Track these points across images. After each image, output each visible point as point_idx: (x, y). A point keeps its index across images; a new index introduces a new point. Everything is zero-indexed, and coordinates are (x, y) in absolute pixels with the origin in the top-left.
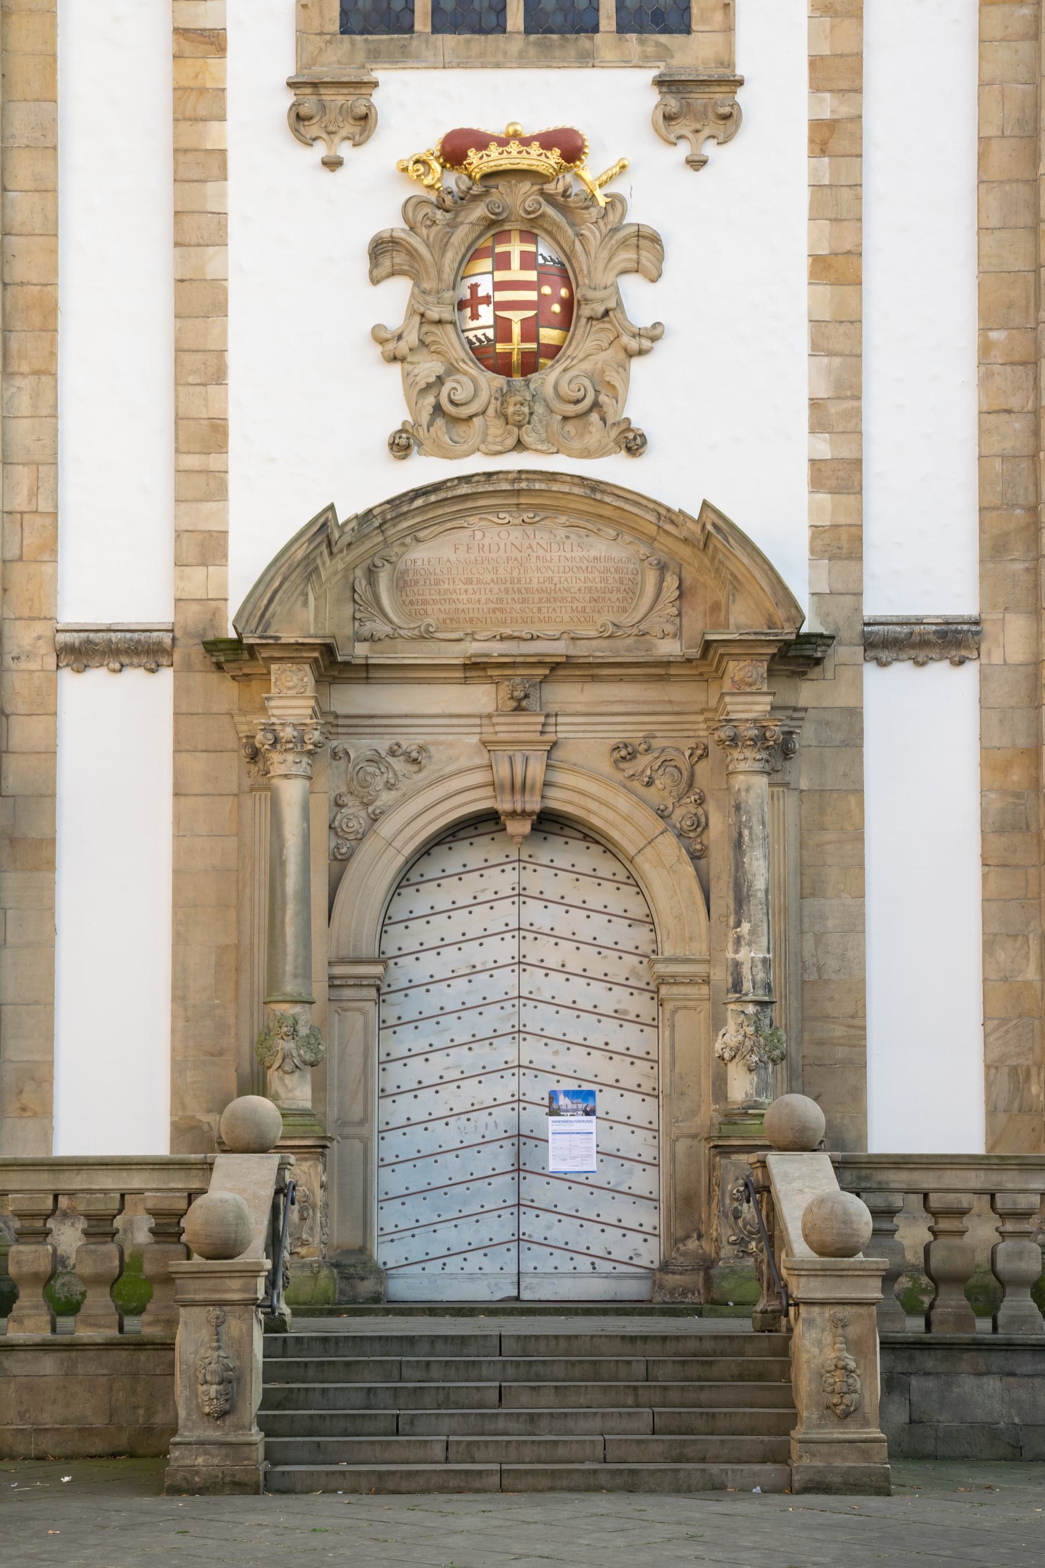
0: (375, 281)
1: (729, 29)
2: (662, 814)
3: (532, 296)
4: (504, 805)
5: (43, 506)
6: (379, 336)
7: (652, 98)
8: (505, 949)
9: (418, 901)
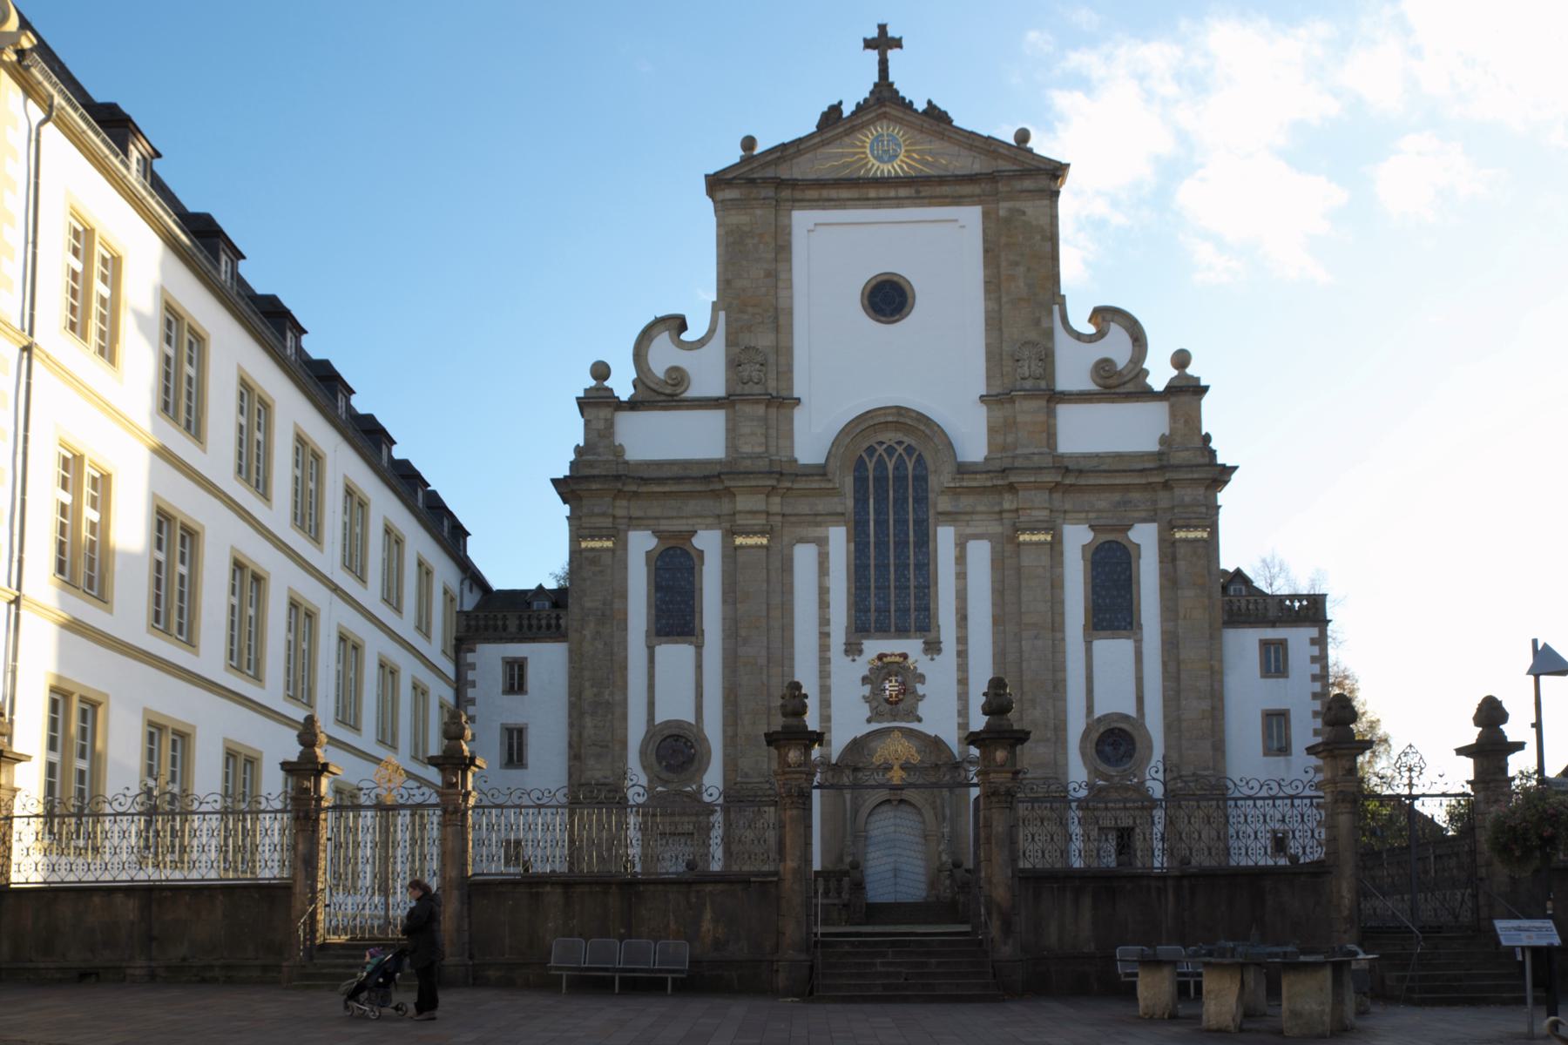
1: (939, 631)
2: (926, 800)
4: (892, 798)
6: (864, 697)
8: (892, 829)
9: (873, 819)
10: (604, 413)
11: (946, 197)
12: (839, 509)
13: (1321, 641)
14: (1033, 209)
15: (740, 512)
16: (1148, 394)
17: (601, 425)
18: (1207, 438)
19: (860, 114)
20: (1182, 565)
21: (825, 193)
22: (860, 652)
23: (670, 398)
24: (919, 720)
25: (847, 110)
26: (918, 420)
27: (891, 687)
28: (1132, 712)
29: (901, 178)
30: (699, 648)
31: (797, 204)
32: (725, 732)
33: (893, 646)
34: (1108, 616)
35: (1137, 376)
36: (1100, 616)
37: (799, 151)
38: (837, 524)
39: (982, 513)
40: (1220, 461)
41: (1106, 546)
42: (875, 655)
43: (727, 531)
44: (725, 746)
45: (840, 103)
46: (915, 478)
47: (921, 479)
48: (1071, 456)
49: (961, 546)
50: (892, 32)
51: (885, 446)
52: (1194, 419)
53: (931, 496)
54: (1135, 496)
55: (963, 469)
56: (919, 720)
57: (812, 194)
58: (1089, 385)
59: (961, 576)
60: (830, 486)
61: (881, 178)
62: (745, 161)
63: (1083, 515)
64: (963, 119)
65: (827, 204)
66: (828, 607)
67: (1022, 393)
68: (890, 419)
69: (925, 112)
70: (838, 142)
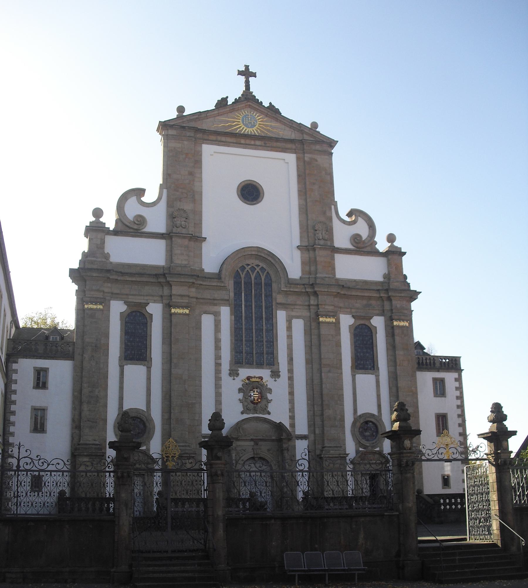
0: (239, 393)
3: (258, 396)
5: (200, 419)
6: (239, 400)
7: (270, 373)
10: (100, 235)
11: (279, 148)
12: (226, 297)
13: (459, 380)
14: (321, 159)
15: (174, 295)
16: (376, 253)
17: (99, 242)
18: (405, 277)
19: (237, 104)
20: (397, 338)
21: (219, 138)
22: (238, 375)
23: (136, 231)
24: (269, 413)
25: (230, 101)
26: (269, 255)
27: (255, 394)
28: (375, 412)
29: (256, 136)
30: (149, 368)
31: (204, 141)
32: (163, 416)
33: (255, 372)
34: (362, 362)
35: (371, 244)
36: (359, 362)
37: (207, 116)
38: (224, 305)
39: (300, 305)
40: (412, 288)
41: (360, 326)
42: (245, 377)
43: (166, 304)
44: (163, 424)
45: (227, 97)
46: (266, 284)
47: (269, 285)
48: (342, 280)
49: (289, 322)
50: (251, 69)
51: (250, 266)
52: (399, 267)
53: (274, 295)
54: (373, 302)
55: (290, 282)
56: (269, 413)
57: (213, 137)
58: (350, 246)
59: (290, 337)
60: (222, 285)
61: (247, 135)
62: (178, 117)
63: (349, 310)
64: (284, 113)
65: (220, 143)
66: (220, 349)
67: (320, 246)
68: (253, 253)
69: (268, 107)
70: (226, 115)
